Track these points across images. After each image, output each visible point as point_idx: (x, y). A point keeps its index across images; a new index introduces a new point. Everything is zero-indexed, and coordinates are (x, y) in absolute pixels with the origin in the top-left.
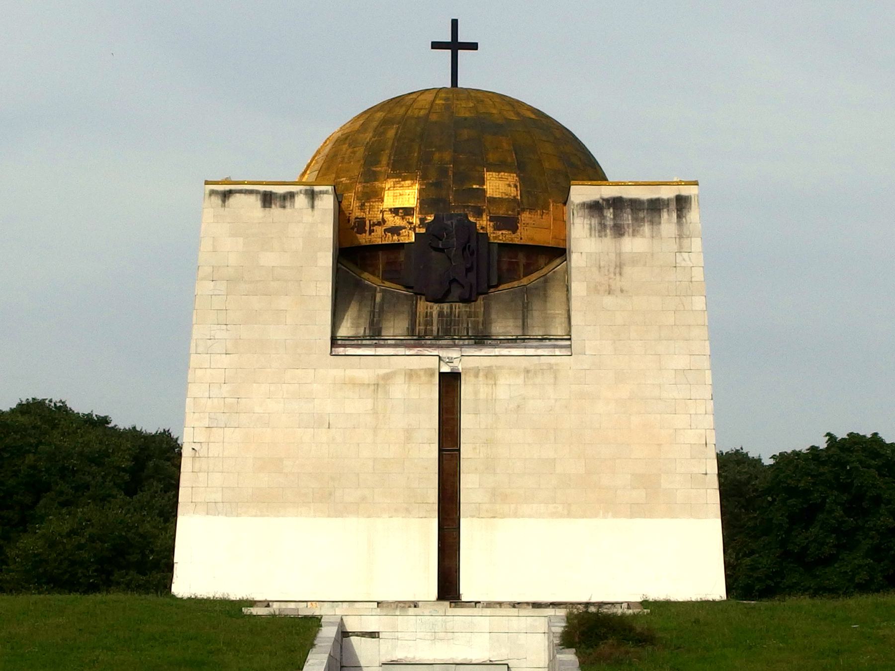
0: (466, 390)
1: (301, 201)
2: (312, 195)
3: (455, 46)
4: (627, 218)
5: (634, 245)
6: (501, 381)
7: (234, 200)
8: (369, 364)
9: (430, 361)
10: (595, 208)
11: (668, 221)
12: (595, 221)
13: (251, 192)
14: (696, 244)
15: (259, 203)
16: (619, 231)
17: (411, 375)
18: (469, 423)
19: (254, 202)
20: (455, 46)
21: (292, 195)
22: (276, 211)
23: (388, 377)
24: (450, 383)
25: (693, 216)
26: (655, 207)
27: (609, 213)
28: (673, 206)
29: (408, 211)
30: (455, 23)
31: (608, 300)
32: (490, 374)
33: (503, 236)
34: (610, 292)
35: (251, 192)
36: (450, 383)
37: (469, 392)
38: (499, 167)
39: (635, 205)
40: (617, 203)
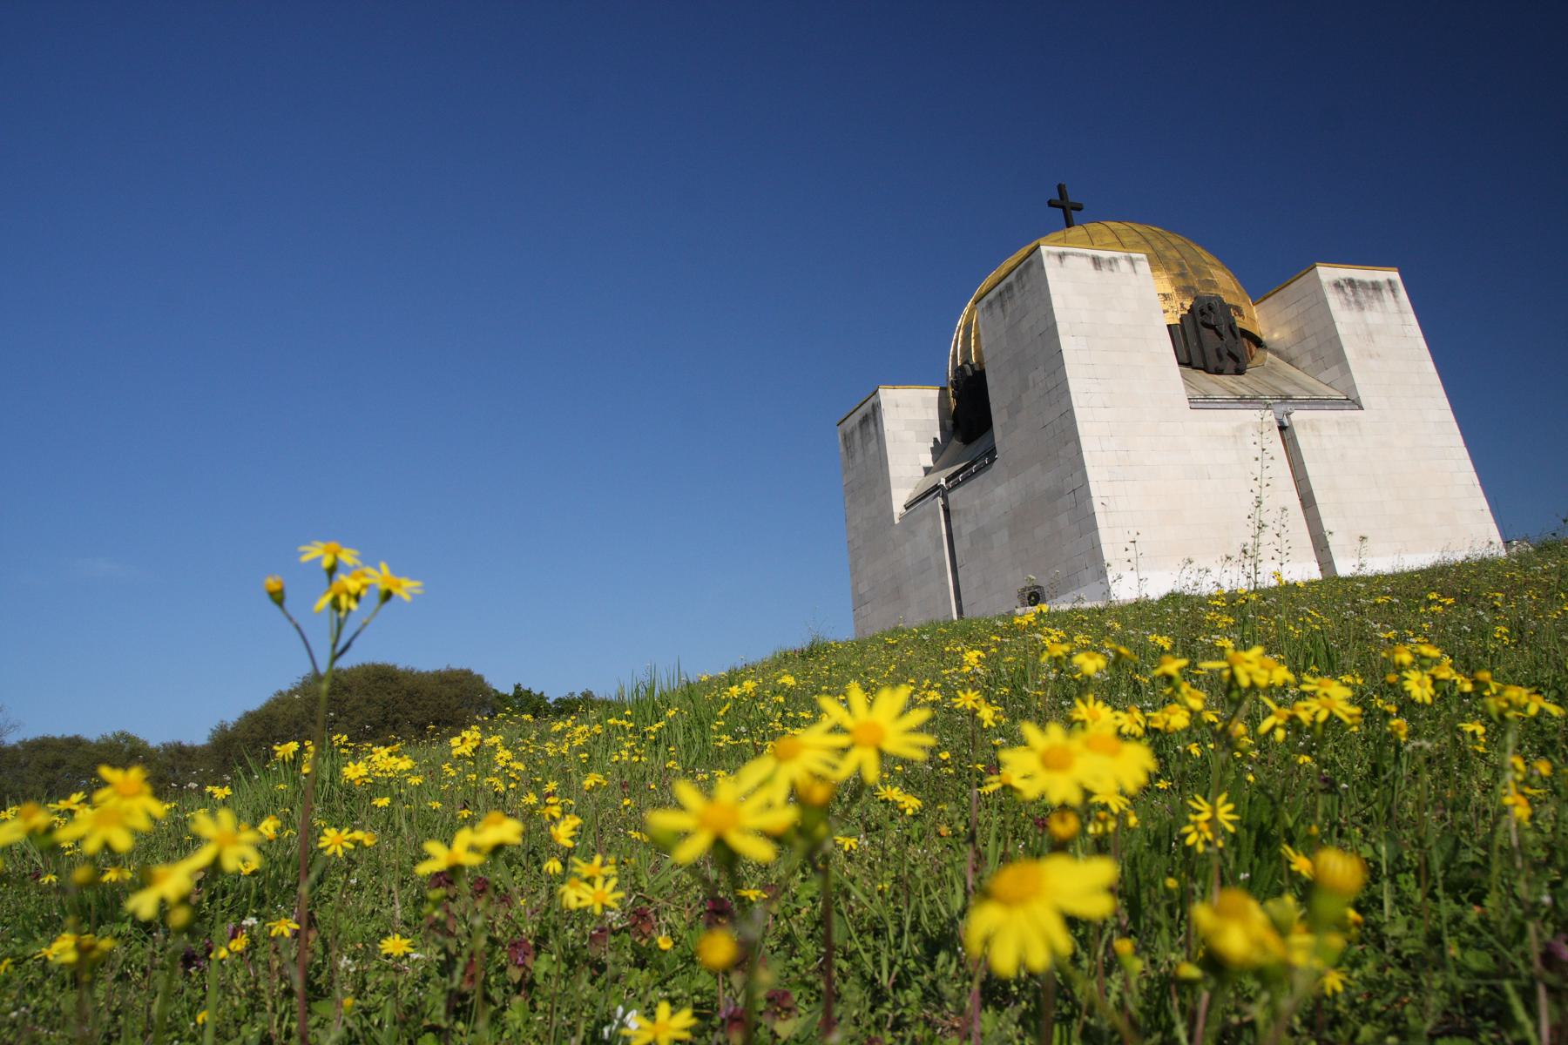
0: (1303, 439)
1: (1124, 265)
2: (1132, 261)
7: (1069, 260)
10: (1337, 285)
12: (1342, 296)
13: (1082, 255)
15: (1091, 266)
21: (1115, 260)
23: (1241, 429)
26: (1376, 287)
27: (1348, 290)
28: (1387, 287)
30: (1061, 188)
32: (1313, 427)
34: (1371, 356)
35: (1082, 255)
39: (1363, 284)
40: (1351, 282)
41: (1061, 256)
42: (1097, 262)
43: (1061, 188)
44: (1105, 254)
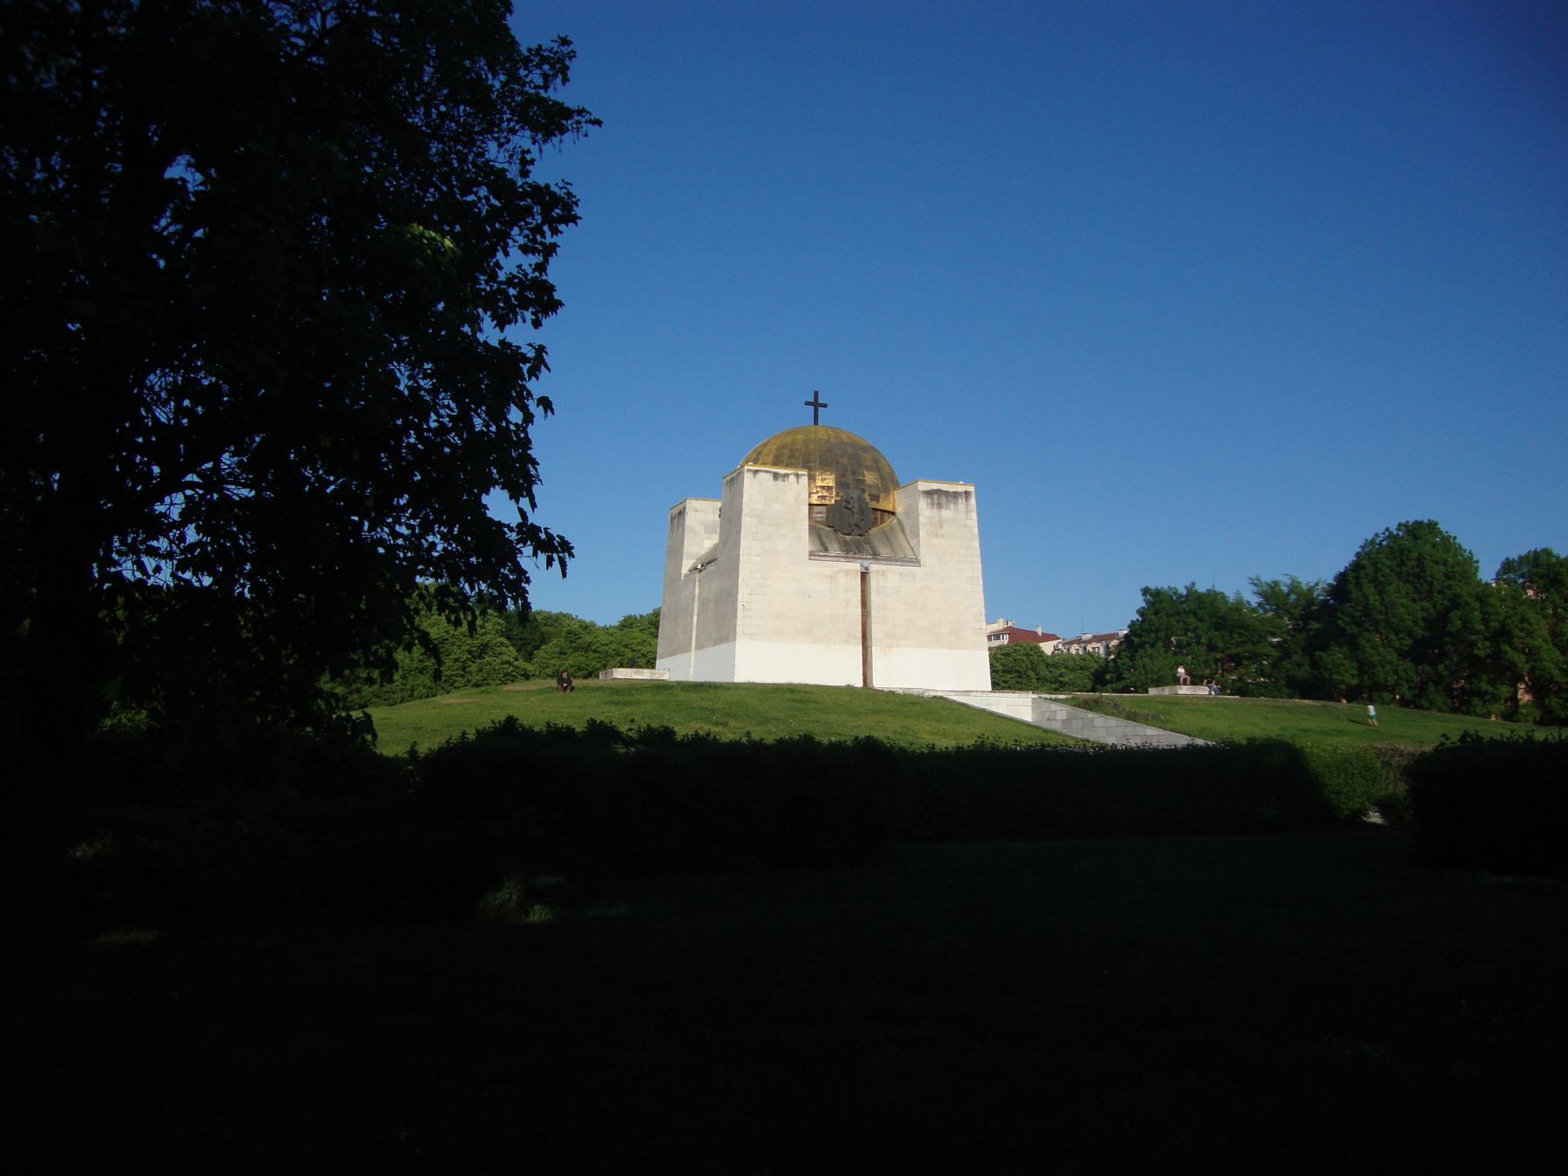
1: (792, 478)
2: (797, 476)
3: (816, 404)
4: (943, 500)
5: (947, 513)
6: (885, 576)
8: (827, 567)
9: (855, 567)
10: (929, 493)
11: (961, 501)
14: (974, 515)
16: (940, 506)
17: (847, 572)
18: (875, 599)
19: (769, 477)
20: (816, 404)
22: (780, 482)
24: (864, 576)
25: (973, 501)
26: (956, 495)
29: (829, 488)
30: (816, 394)
31: (936, 541)
33: (873, 505)
36: (864, 576)
37: (873, 581)
38: (868, 469)
39: (946, 493)
40: (939, 492)
41: (756, 472)
42: (776, 476)
43: (816, 394)
44: (782, 471)
